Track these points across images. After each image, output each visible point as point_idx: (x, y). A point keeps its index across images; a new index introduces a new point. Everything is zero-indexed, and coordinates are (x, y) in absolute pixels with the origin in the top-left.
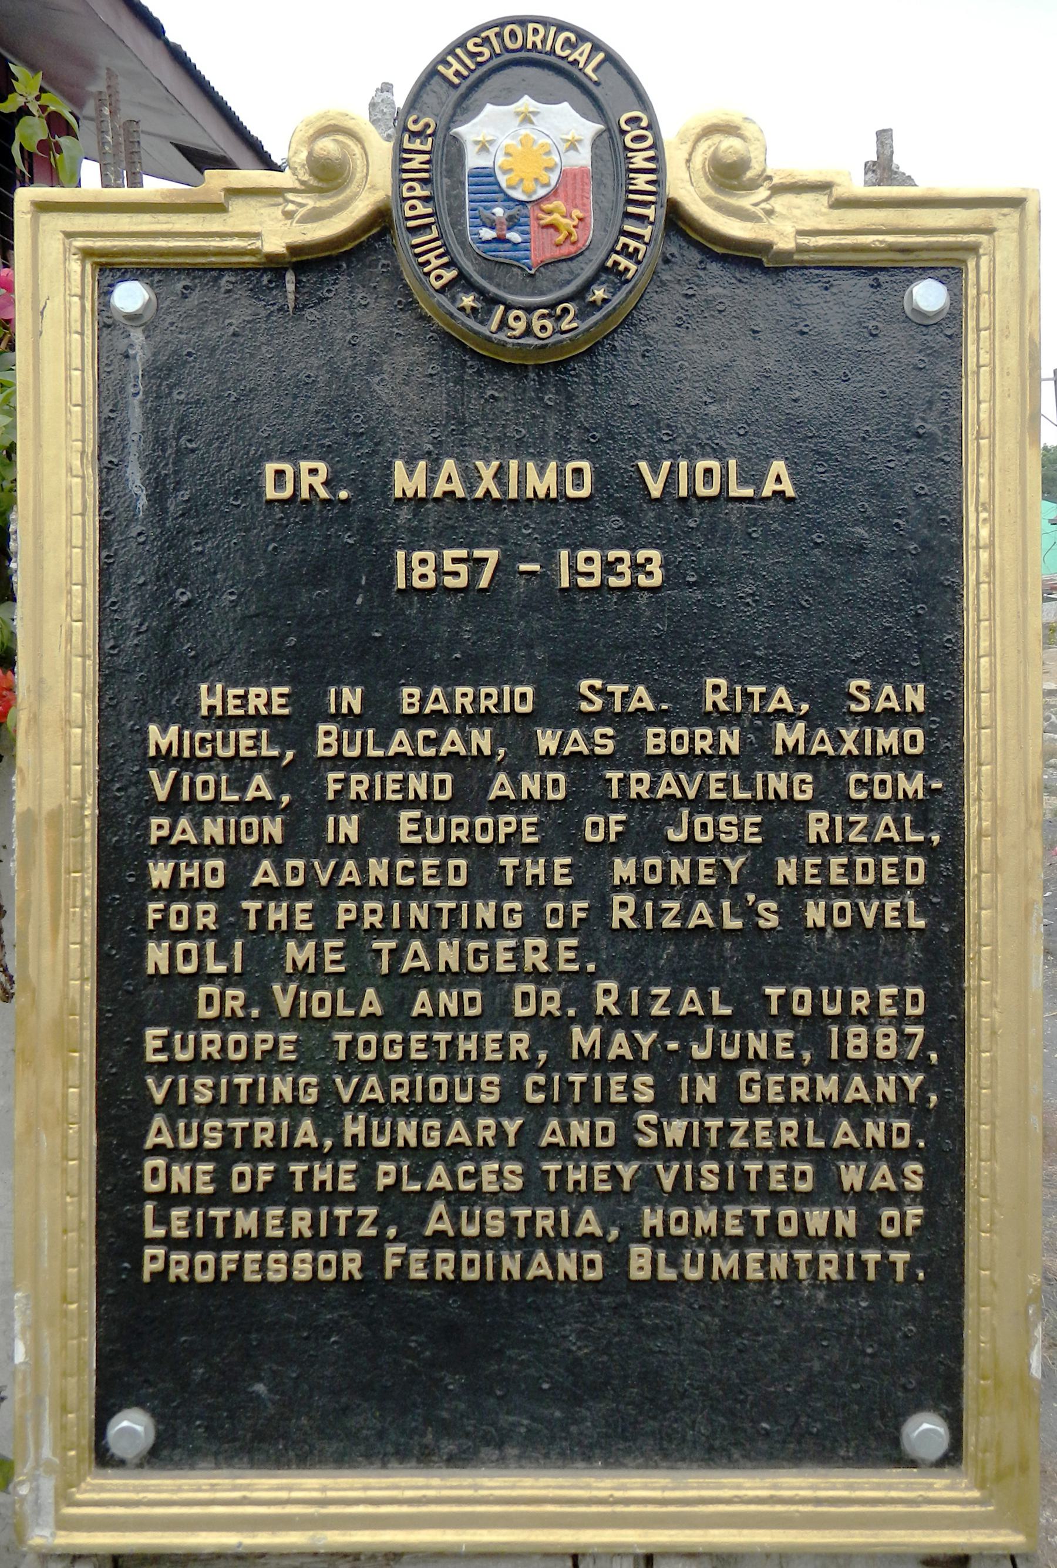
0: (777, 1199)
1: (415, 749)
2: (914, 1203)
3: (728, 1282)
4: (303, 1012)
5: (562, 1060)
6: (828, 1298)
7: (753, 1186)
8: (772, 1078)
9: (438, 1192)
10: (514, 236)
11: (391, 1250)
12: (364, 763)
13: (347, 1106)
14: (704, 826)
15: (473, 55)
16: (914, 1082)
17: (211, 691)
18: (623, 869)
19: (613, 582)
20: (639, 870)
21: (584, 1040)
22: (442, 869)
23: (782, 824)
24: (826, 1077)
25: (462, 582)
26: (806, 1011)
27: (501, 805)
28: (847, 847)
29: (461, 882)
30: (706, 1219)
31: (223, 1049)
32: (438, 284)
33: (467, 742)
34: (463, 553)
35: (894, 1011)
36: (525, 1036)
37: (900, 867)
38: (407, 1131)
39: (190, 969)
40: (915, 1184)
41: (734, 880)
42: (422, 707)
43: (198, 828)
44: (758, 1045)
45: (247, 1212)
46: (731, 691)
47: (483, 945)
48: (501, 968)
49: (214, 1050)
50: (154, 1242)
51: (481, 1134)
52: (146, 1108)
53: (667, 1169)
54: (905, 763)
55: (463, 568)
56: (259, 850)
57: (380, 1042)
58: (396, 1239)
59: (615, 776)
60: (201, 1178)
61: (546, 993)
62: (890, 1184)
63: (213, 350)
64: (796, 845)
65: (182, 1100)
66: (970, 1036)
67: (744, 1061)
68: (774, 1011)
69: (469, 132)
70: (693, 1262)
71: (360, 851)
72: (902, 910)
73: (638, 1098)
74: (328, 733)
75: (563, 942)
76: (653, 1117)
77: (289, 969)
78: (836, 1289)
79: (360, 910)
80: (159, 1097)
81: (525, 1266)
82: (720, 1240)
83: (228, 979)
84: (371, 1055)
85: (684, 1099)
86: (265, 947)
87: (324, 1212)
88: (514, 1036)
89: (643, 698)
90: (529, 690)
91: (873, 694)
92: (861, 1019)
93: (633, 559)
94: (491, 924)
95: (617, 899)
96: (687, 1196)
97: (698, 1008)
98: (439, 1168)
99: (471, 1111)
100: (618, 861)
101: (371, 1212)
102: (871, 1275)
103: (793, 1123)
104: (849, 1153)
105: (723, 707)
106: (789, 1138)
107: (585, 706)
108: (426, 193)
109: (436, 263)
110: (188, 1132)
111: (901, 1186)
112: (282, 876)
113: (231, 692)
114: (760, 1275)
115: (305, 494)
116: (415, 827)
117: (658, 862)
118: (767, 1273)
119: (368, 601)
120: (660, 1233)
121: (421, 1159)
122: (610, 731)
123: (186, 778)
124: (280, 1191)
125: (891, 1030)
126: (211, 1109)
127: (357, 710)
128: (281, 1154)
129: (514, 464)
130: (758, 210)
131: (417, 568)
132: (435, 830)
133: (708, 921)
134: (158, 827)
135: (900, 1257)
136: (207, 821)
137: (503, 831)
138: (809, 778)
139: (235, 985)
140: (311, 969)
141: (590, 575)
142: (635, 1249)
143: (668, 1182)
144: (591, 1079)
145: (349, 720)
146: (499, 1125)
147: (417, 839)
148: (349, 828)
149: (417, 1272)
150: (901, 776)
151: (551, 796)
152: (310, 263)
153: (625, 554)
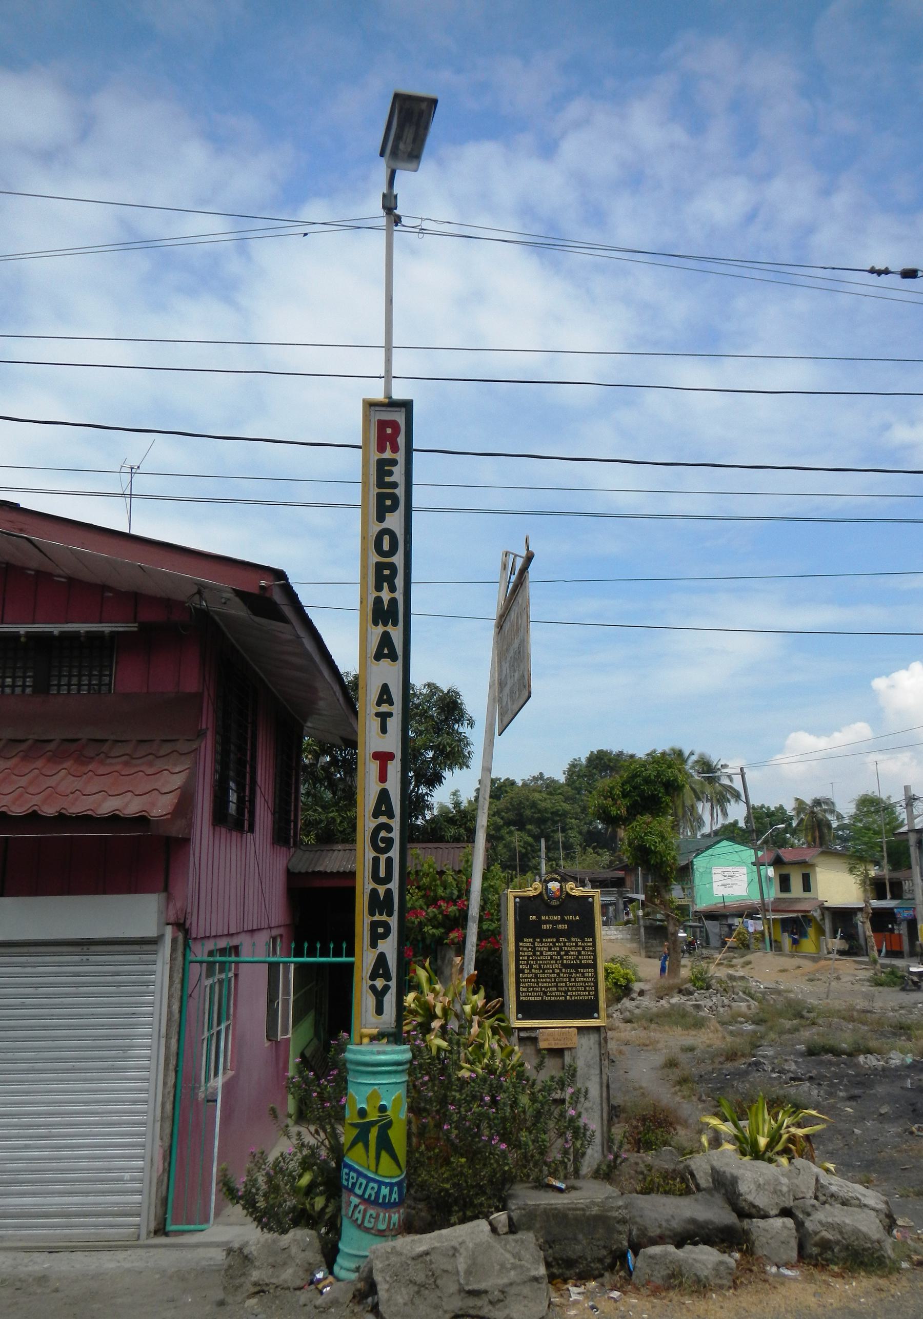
86: (531, 966)
121: (546, 987)
124: (533, 991)
131: (544, 927)
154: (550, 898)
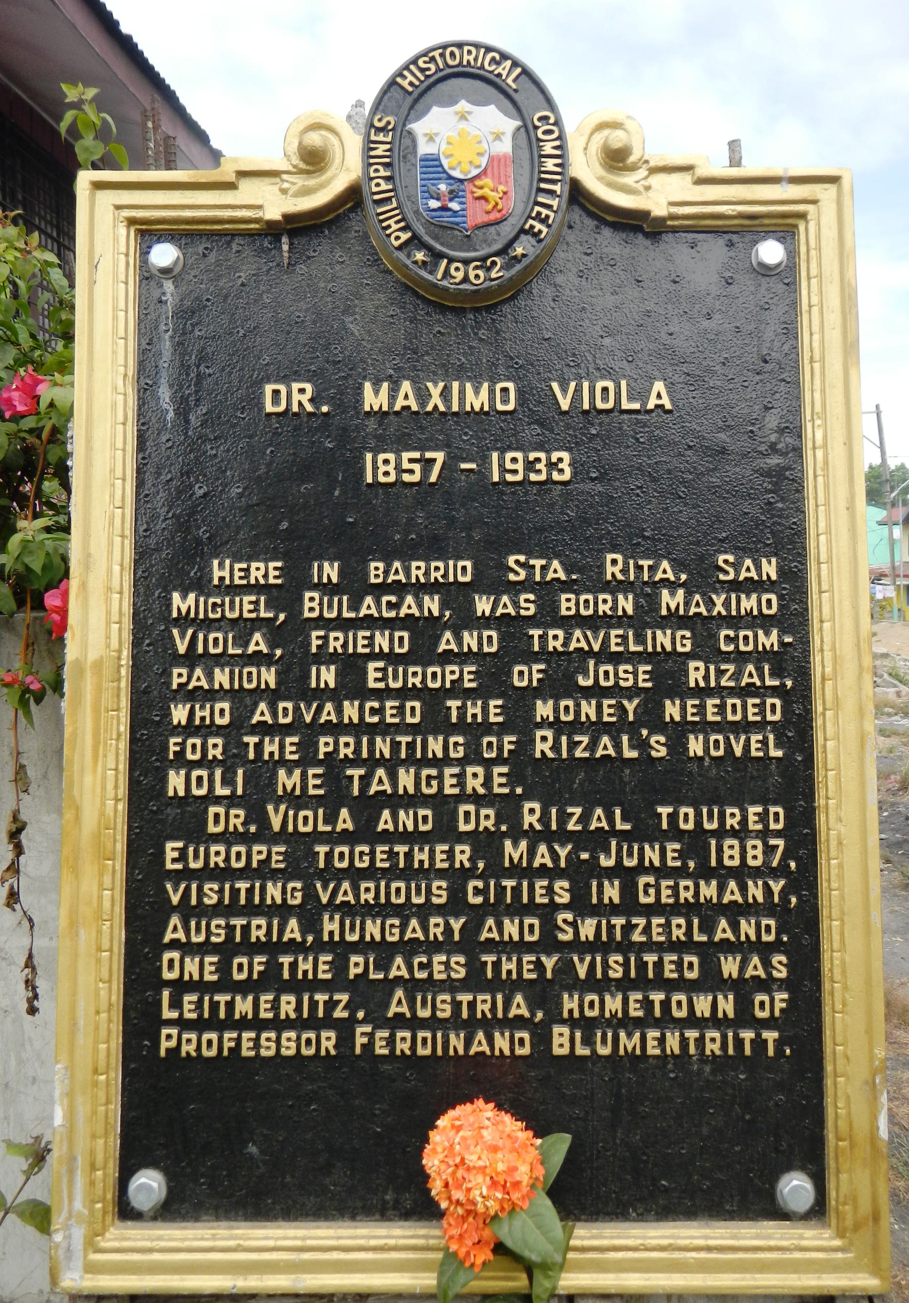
0: (670, 986)
1: (380, 612)
2: (780, 989)
3: (631, 1056)
4: (291, 828)
5: (496, 870)
6: (713, 1072)
7: (651, 975)
8: (664, 883)
9: (399, 979)
10: (454, 206)
11: (359, 1030)
12: (341, 624)
13: (325, 907)
14: (606, 673)
15: (422, 70)
16: (777, 887)
17: (221, 566)
18: (544, 709)
19: (533, 477)
20: (556, 710)
21: (514, 851)
22: (401, 710)
23: (668, 674)
24: (708, 884)
25: (416, 478)
26: (690, 826)
27: (447, 657)
28: (720, 691)
29: (417, 720)
30: (613, 1004)
31: (227, 859)
32: (396, 244)
33: (420, 606)
34: (416, 455)
35: (759, 827)
36: (467, 848)
37: (761, 707)
38: (373, 929)
39: (203, 792)
40: (781, 973)
41: (631, 718)
42: (385, 578)
43: (210, 677)
44: (652, 855)
45: (244, 998)
46: (626, 564)
47: (434, 772)
48: (448, 791)
49: (220, 860)
50: (170, 1023)
51: (432, 930)
52: (165, 909)
53: (582, 960)
54: (763, 622)
55: (417, 467)
56: (259, 693)
57: (352, 853)
58: (364, 1021)
59: (536, 633)
60: (208, 968)
61: (483, 812)
62: (761, 973)
63: (226, 297)
64: (681, 691)
65: (194, 902)
66: (822, 847)
67: (641, 869)
68: (665, 826)
69: (419, 127)
70: (604, 1041)
71: (336, 696)
72: (764, 742)
73: (558, 900)
74: (312, 599)
75: (497, 770)
76: (570, 917)
77: (280, 793)
78: (720, 1062)
79: (336, 743)
80: (175, 899)
81: (468, 1044)
82: (624, 1022)
83: (231, 801)
84: (345, 864)
85: (595, 901)
86: (262, 774)
87: (306, 998)
88: (458, 848)
89: (557, 570)
90: (468, 564)
91: (737, 566)
92: (734, 833)
93: (549, 459)
94: (440, 755)
95: (539, 734)
96: (598, 984)
97: (604, 824)
98: (399, 960)
99: (425, 912)
100: (539, 703)
101: (344, 997)
102: (748, 1051)
103: (682, 921)
104: (727, 947)
105: (620, 577)
106: (678, 934)
107: (512, 577)
108: (388, 174)
109: (395, 227)
110: (198, 930)
111: (769, 974)
112: (274, 714)
113: (237, 566)
114: (657, 1052)
115: (295, 408)
116: (379, 675)
117: (571, 703)
118: (663, 1050)
119: (343, 493)
120: (576, 1015)
121: (384, 952)
122: (531, 597)
123: (201, 636)
124: (270, 981)
125: (759, 843)
126: (218, 910)
127: (335, 580)
128: (272, 948)
129: (456, 385)
130: (639, 187)
131: (381, 467)
132: (395, 677)
133: (611, 752)
134: (178, 676)
135: (771, 1036)
136: (217, 671)
137: (449, 678)
138: (688, 634)
139: (237, 806)
140: (298, 792)
141: (515, 472)
142: (556, 1029)
143: (582, 972)
144: (520, 885)
145: (329, 589)
146: (447, 924)
147: (381, 685)
148: (328, 676)
149: (381, 1050)
150: (760, 633)
151: (486, 649)
152: (298, 227)
153: (542, 455)
154: (439, 236)
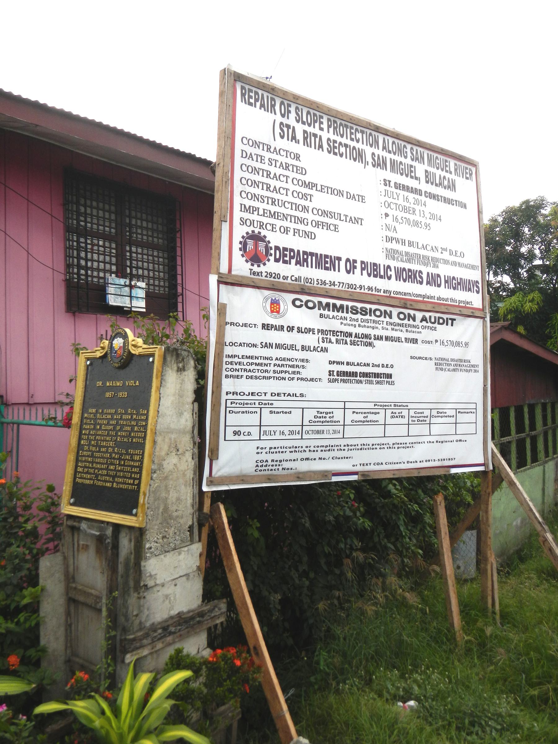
86: (91, 440)
121: (99, 469)
124: (87, 473)
152: (100, 357)
